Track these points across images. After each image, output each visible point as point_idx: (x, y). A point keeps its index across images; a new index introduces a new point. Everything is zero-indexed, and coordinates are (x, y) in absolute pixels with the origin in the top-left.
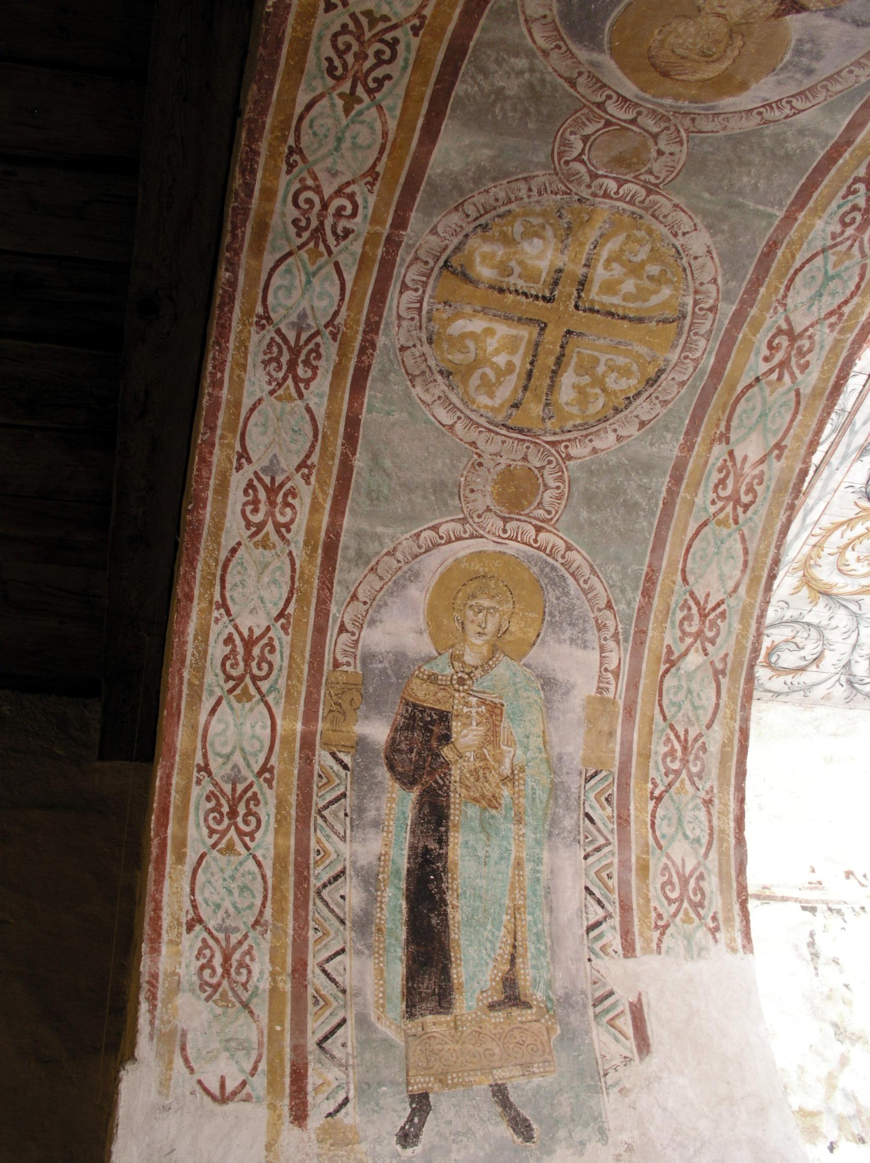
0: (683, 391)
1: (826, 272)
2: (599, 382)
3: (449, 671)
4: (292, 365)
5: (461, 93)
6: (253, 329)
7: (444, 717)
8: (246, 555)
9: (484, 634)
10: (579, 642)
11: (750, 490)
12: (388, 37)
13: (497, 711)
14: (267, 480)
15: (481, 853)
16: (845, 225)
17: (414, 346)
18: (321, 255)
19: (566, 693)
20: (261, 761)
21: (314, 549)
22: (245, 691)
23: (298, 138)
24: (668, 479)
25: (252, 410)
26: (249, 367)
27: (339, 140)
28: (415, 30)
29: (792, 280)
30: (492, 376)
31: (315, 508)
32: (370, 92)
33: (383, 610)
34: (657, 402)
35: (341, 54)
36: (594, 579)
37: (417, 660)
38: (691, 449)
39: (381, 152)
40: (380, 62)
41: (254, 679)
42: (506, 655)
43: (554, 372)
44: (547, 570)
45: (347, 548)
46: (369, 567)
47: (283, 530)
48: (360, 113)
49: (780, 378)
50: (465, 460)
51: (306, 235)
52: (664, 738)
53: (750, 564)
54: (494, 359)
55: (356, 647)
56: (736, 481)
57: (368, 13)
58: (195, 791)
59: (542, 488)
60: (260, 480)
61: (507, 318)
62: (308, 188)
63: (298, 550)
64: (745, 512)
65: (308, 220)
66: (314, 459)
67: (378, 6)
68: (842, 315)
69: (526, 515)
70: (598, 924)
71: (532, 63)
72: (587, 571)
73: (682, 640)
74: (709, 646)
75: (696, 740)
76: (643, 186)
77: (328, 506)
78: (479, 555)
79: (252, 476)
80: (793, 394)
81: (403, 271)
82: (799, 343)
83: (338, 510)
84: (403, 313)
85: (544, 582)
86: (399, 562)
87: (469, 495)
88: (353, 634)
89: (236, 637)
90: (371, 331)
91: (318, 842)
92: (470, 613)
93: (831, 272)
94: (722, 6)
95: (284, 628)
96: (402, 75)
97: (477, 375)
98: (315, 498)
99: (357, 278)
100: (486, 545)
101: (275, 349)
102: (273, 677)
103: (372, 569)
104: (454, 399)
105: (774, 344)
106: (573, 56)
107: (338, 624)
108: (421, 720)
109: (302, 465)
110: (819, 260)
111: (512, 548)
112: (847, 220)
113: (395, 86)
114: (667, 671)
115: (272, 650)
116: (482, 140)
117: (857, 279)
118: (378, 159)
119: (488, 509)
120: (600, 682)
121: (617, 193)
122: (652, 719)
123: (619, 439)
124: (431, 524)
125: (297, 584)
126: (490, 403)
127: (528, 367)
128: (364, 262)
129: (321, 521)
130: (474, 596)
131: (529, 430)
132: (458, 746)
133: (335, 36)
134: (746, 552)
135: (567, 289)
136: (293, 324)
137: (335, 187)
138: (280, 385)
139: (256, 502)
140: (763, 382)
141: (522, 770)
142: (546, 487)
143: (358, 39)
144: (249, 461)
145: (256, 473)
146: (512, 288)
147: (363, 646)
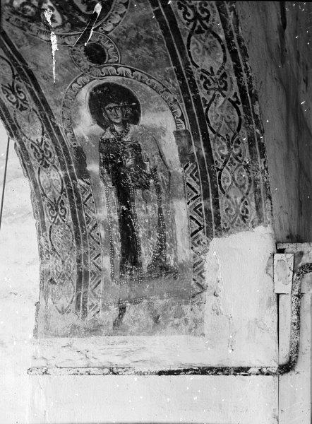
3: (112, 137)
11: (203, 11)
14: (7, 85)
15: (144, 209)
20: (61, 188)
21: (40, 105)
22: (46, 163)
41: (47, 158)
45: (50, 101)
50: (67, 51)
53: (226, 46)
58: (44, 203)
64: (207, 22)
70: (196, 231)
74: (224, 92)
75: (233, 138)
77: (33, 88)
78: (100, 87)
91: (86, 215)
92: (108, 111)
102: (53, 156)
109: (14, 76)
111: (111, 79)
114: (207, 110)
115: (48, 146)
123: (121, 16)
141: (155, 170)
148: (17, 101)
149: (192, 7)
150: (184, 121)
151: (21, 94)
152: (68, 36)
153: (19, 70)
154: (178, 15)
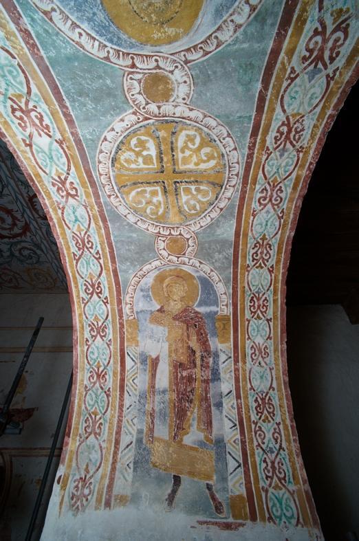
0: (97, 159)
2: (138, 154)
4: (289, 131)
11: (21, 118)
12: (255, 261)
16: (89, 242)
17: (230, 151)
18: (272, 181)
23: (280, 222)
24: (72, 113)
25: (317, 106)
26: (311, 127)
27: (267, 225)
28: (248, 266)
29: (89, 216)
30: (190, 145)
31: (291, 53)
32: (258, 242)
36: (76, 37)
38: (72, 133)
39: (252, 224)
40: (256, 253)
43: (162, 153)
44: (115, 40)
49: (59, 177)
50: (193, 99)
51: (278, 188)
56: (33, 121)
57: (262, 268)
59: (142, 91)
65: (277, 194)
66: (285, 84)
69: (146, 74)
72: (84, 40)
77: (282, 54)
78: (171, 40)
79: (329, 66)
82: (65, 193)
83: (275, 53)
84: (237, 165)
85: (113, 28)
86: (232, 21)
93: (78, 222)
97: (196, 146)
99: (257, 175)
100: (166, 49)
101: (297, 137)
103: (254, 10)
106: (204, 272)
109: (293, 80)
110: (87, 227)
111: (147, 51)
112: (90, 244)
118: (253, 221)
119: (172, 72)
124: (209, 55)
126: (187, 132)
127: (174, 153)
129: (289, 43)
131: (162, 123)
133: (270, 258)
135: (171, 188)
136: (286, 151)
138: (298, 121)
139: (332, 50)
140: (65, 174)
143: (263, 258)
144: (328, 76)
149: (35, 125)
151: (311, 46)
152: (183, 118)
154: (50, 119)
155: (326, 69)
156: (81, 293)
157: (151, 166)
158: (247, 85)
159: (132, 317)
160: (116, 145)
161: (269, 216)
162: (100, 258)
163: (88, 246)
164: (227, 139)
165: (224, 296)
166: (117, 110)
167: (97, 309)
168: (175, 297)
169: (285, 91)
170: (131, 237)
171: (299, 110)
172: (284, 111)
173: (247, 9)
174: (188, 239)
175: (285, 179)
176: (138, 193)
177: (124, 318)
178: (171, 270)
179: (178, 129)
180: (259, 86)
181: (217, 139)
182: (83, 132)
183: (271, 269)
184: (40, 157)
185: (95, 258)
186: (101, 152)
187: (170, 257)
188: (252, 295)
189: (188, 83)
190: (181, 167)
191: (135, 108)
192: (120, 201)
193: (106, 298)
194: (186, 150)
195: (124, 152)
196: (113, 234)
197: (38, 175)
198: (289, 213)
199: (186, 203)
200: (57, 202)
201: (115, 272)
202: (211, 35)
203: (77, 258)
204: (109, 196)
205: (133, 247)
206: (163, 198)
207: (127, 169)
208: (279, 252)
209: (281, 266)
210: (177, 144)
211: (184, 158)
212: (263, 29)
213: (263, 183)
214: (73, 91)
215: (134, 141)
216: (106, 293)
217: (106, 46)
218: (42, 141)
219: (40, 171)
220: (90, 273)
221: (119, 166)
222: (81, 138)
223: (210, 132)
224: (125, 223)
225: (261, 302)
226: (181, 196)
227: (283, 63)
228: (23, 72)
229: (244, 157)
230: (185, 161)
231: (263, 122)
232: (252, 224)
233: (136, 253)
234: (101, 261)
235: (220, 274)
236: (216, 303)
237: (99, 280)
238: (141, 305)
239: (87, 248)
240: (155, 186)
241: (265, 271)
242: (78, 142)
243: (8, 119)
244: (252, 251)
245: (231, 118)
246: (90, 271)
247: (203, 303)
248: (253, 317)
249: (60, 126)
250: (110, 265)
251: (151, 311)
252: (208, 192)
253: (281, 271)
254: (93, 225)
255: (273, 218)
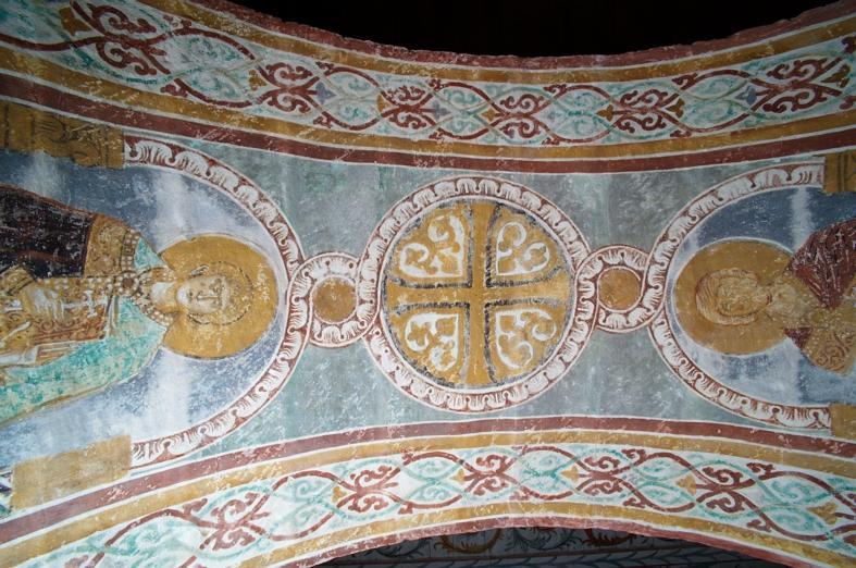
0: (440, 409)
1: (556, 470)
2: (435, 342)
4: (406, 108)
5: (633, 177)
6: (429, 78)
7: (73, 267)
8: (241, 63)
9: (191, 300)
10: (196, 404)
11: (369, 502)
12: (664, 120)
13: (92, 332)
18: (491, 120)
19: (128, 408)
21: (255, 126)
23: (571, 89)
24: (365, 428)
25: (368, 78)
26: (400, 77)
28: (677, 133)
29: (545, 448)
30: (423, 259)
31: (295, 128)
32: (618, 123)
33: (203, 192)
34: (427, 392)
35: (642, 98)
36: (264, 396)
37: (148, 230)
38: (395, 436)
39: (575, 141)
40: (642, 123)
42: (168, 328)
43: (436, 304)
44: (268, 348)
46: (245, 177)
47: (270, 99)
48: (601, 121)
49: (467, 478)
51: (503, 107)
52: (79, 556)
53: (305, 538)
54: (436, 257)
55: (155, 162)
56: (373, 487)
57: (681, 103)
60: (312, 82)
61: (469, 258)
62: (537, 103)
63: (252, 111)
64: (350, 508)
65: (515, 106)
66: (336, 128)
67: (689, 107)
68: (526, 498)
69: (314, 316)
71: (671, 209)
72: (269, 385)
73: (215, 512)
76: (594, 314)
77: (297, 139)
78: (272, 280)
79: (315, 75)
80: (456, 495)
81: (491, 177)
82: (496, 478)
83: (295, 148)
84: (460, 182)
85: (255, 348)
86: (254, 205)
87: (324, 261)
88: (172, 160)
89: (150, 36)
90: (442, 162)
93: (557, 473)
94: (780, 296)
95: (169, 88)
96: (635, 138)
98: (304, 128)
99: (480, 146)
100: (282, 286)
101: (416, 95)
103: (244, 180)
104: (399, 235)
105: (492, 461)
106: (688, 231)
107: (182, 145)
108: (68, 239)
109: (330, 118)
110: (569, 459)
112: (605, 462)
113: (627, 137)
114: (175, 513)
116: (602, 199)
117: (557, 494)
118: (569, 141)
119: (313, 281)
120: (151, 443)
121: (584, 300)
122: (107, 526)
125: (219, 107)
127: (436, 285)
128: (492, 149)
129: (283, 132)
130: (230, 282)
131: (385, 299)
132: (28, 289)
133: (655, 92)
134: (314, 529)
136: (438, 106)
137: (540, 119)
138: (390, 99)
139: (294, 77)
140: (461, 467)
142: (340, 327)
144: (327, 74)
145: (317, 79)
146: (492, 255)
147: (159, 171)
148: (273, 81)
149: (379, 486)
150: (159, 460)
151: (289, 104)
153: (338, 137)
154: (372, 462)
155: (317, 79)
156: (735, 523)
157: (456, 323)
158: (334, 178)
159: (821, 413)
160: (418, 374)
161: (561, 112)
162: (641, 452)
163: (611, 467)
164: (415, 200)
165: (760, 179)
166: (362, 361)
167: (791, 501)
168: (756, 299)
169: (345, 126)
170: (595, 378)
171: (373, 101)
172: (374, 122)
173: (243, 189)
174: (606, 265)
175: (487, 98)
176: (505, 351)
177: (826, 437)
178: (679, 304)
179: (396, 276)
180: (337, 163)
181: (415, 217)
182: (394, 419)
183: (686, 81)
184: (430, 498)
185: (640, 462)
186: (427, 399)
187: (646, 303)
188: (760, 110)
189: (328, 259)
190: (461, 274)
191: (361, 336)
192: (520, 386)
193: (755, 468)
194: (432, 265)
195: (430, 363)
196: (587, 412)
197: (461, 512)
198: (554, 75)
199: (528, 266)
200: (512, 498)
201: (678, 428)
202: (269, 230)
203: (638, 501)
204: (508, 403)
205: (620, 379)
206: (519, 308)
207: (460, 362)
208: (644, 74)
209: (677, 61)
210: (420, 279)
211: (445, 269)
212: (265, 167)
213: (493, 134)
214: (332, 418)
215: (413, 345)
216: (739, 463)
217: (276, 361)
218: (405, 485)
219: (453, 506)
220: (678, 484)
221: (453, 376)
222: (403, 424)
223: (403, 228)
224: (566, 385)
225: (785, 82)
226: (516, 276)
227: (308, 136)
228: (304, 474)
229: (447, 173)
230: (450, 266)
231: (390, 150)
232: (575, 141)
233: (635, 375)
234: (650, 451)
235: (695, 194)
236: (781, 199)
237: (700, 469)
238: (782, 385)
239: (616, 472)
240: (495, 320)
241: (690, 96)
242: (410, 431)
243: (369, 521)
244: (639, 131)
245: (383, 197)
246: (672, 483)
247: (782, 230)
248: (836, 93)
249: (382, 451)
250: (661, 435)
251: (801, 363)
252: (508, 229)
253: (692, 57)
254: (565, 446)
255: (563, 104)
